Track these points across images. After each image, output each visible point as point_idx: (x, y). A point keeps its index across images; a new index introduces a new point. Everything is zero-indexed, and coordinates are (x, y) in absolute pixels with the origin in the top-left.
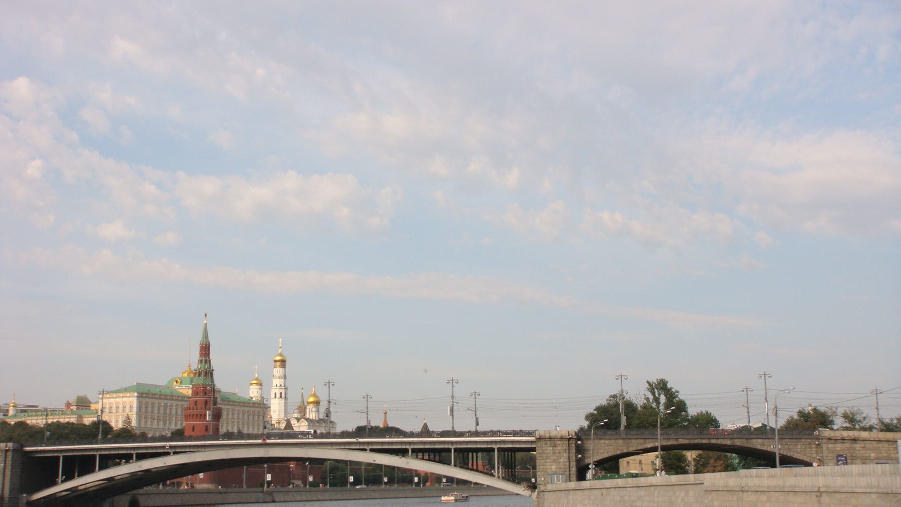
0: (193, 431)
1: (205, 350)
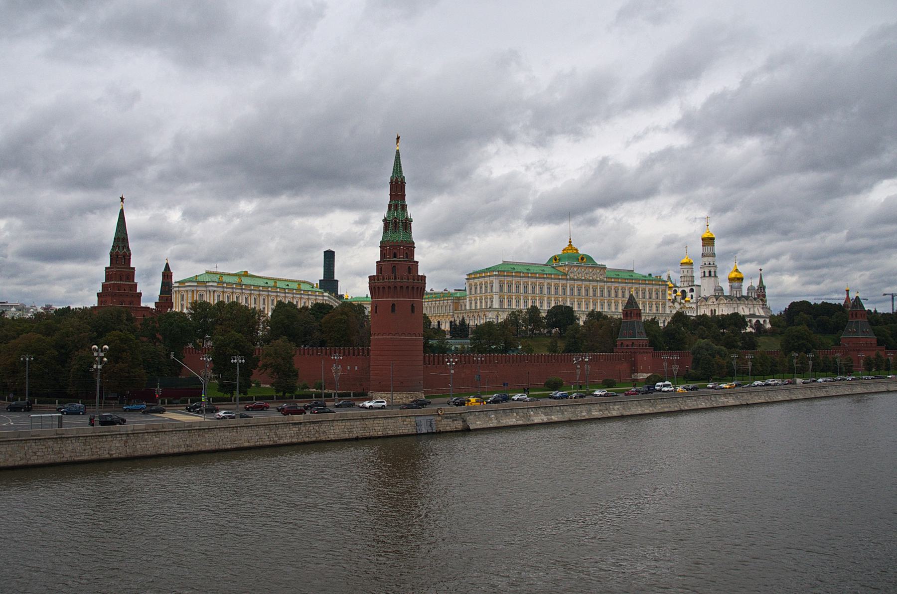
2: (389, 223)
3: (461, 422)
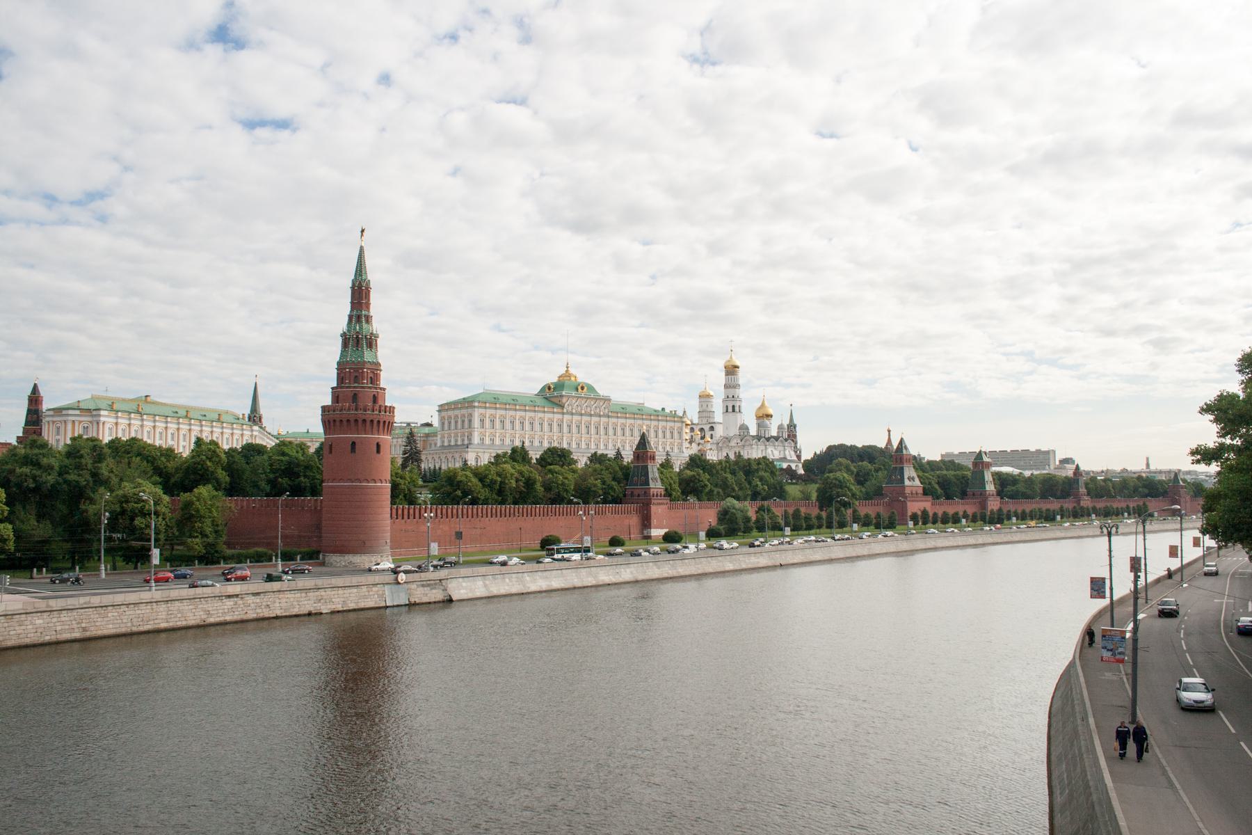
0: (331, 452)
1: (360, 294)
2: (349, 338)
3: (441, 591)
